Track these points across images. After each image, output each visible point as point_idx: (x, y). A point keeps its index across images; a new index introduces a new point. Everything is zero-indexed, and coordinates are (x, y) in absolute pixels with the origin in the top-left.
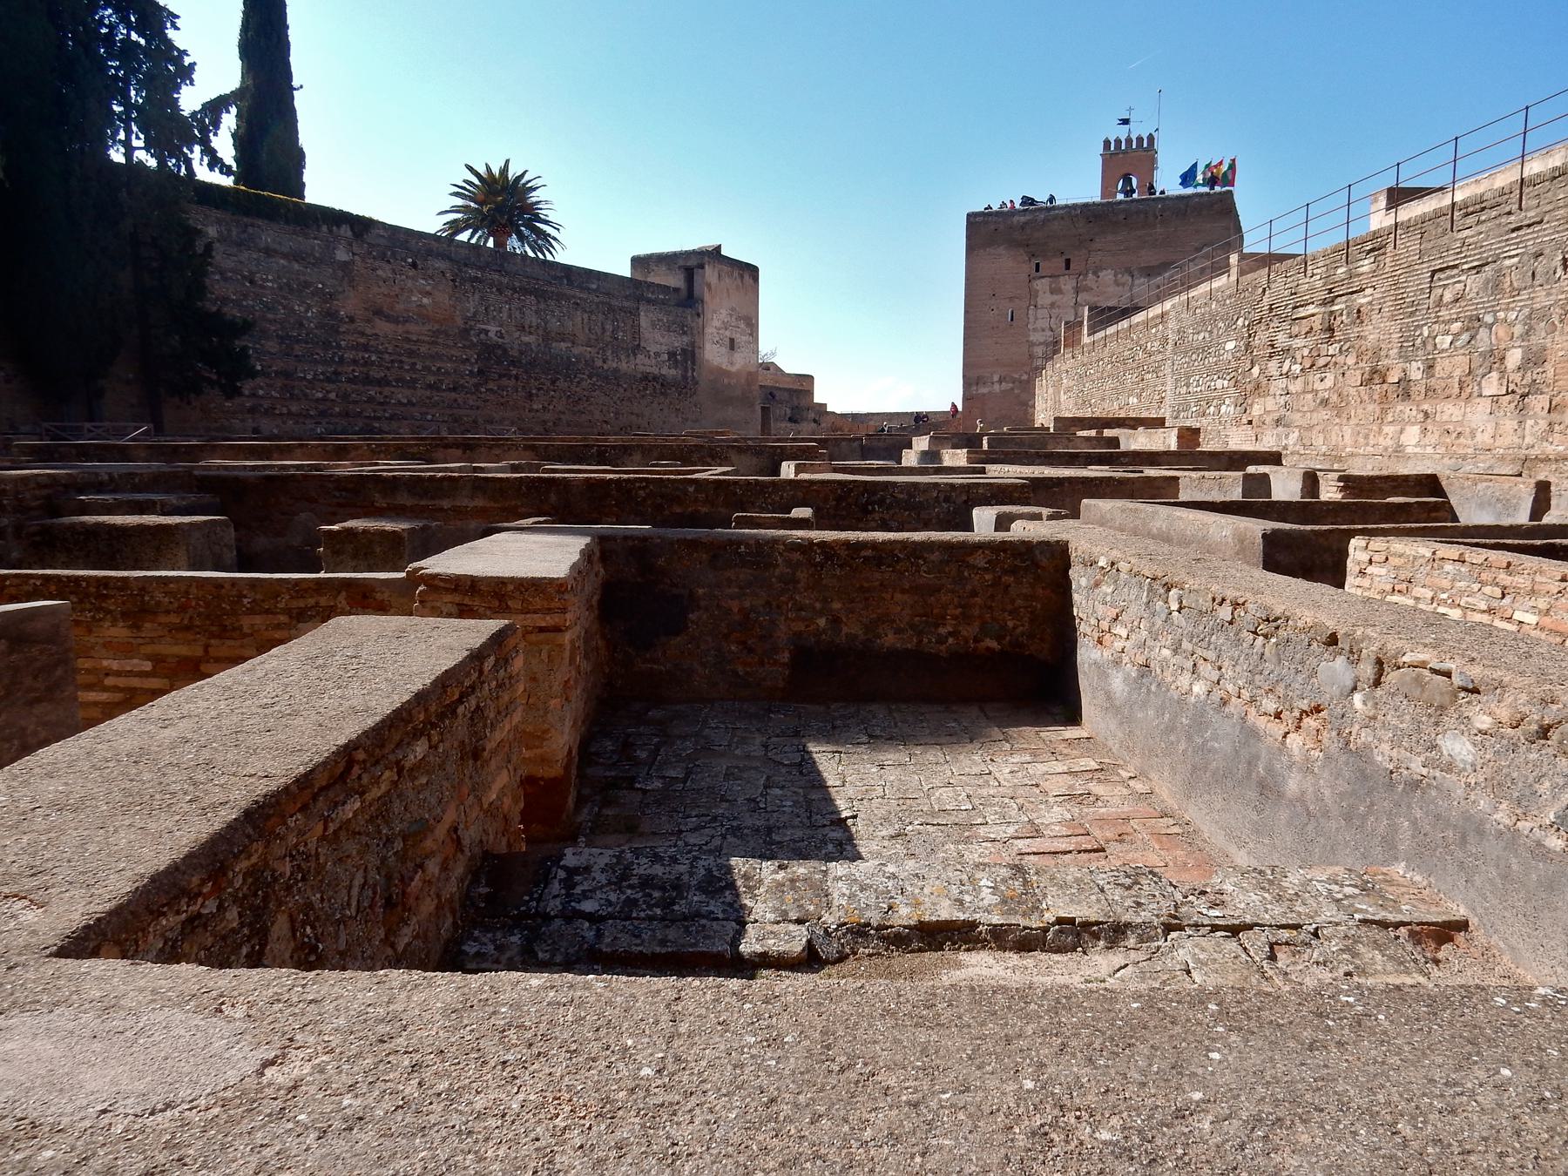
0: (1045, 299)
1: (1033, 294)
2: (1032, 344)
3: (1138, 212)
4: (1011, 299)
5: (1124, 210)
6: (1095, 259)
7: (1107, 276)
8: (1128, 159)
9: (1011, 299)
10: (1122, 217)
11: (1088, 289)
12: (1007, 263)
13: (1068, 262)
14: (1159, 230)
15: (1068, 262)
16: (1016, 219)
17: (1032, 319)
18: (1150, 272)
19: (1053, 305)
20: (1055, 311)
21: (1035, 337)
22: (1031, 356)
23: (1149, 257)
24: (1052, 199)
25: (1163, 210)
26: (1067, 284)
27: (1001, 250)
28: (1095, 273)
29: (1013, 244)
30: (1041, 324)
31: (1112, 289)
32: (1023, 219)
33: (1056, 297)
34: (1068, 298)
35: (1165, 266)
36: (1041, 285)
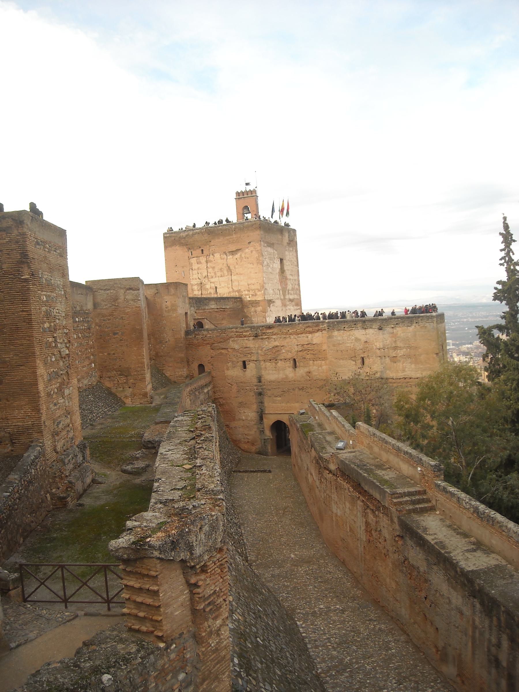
0: (195, 266)
1: (191, 264)
2: (192, 285)
3: (226, 230)
4: (183, 267)
5: (221, 229)
6: (212, 248)
7: (217, 255)
8: (246, 199)
9: (183, 267)
10: (220, 232)
11: (211, 261)
12: (180, 252)
13: (202, 250)
14: (234, 236)
15: (202, 250)
16: (182, 234)
17: (191, 275)
18: (233, 253)
19: (198, 268)
20: (200, 271)
21: (194, 282)
22: (193, 290)
23: (233, 248)
24: (194, 226)
25: (235, 228)
26: (203, 259)
27: (177, 247)
28: (213, 254)
29: (182, 244)
30: (195, 276)
31: (220, 261)
32: (184, 235)
33: (199, 265)
34: (204, 265)
35: (238, 250)
36: (194, 261)
